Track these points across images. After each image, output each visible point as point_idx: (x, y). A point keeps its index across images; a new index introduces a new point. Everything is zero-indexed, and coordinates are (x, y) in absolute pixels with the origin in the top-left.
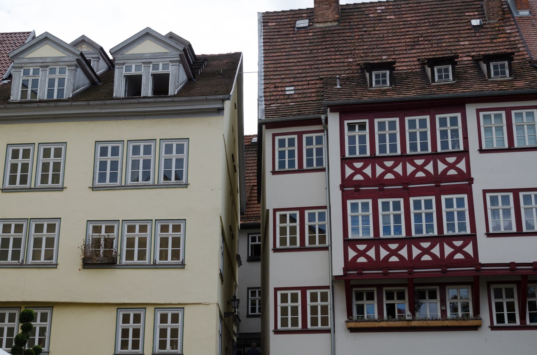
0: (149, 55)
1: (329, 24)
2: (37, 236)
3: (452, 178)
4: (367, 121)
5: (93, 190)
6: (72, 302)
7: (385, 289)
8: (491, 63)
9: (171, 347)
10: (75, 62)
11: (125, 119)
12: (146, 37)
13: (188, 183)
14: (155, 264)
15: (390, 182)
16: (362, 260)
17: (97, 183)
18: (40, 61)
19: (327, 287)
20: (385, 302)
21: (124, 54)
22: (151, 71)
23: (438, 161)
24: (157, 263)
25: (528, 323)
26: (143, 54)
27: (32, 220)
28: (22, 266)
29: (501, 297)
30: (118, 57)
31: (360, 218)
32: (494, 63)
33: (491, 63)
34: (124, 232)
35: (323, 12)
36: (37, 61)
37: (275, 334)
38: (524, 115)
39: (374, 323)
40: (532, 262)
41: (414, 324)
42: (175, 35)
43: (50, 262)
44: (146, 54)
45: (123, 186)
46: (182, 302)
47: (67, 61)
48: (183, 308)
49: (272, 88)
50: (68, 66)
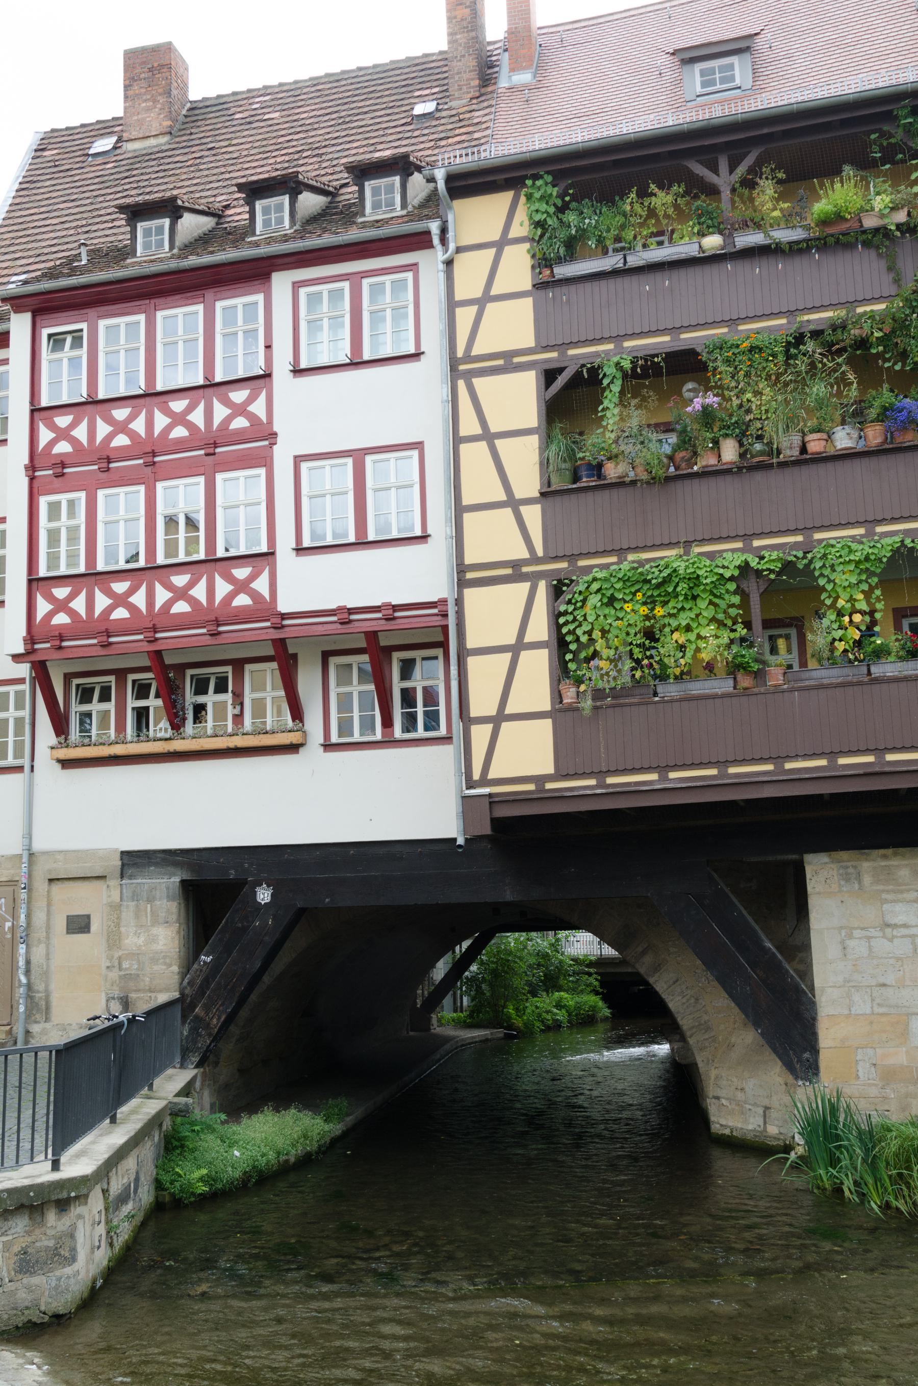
1: (153, 142)
3: (241, 437)
4: (84, 326)
7: (131, 677)
8: (367, 183)
15: (124, 454)
16: (61, 619)
19: (21, 681)
20: (132, 703)
23: (215, 401)
25: (398, 733)
29: (350, 683)
31: (64, 533)
32: (372, 182)
33: (367, 183)
35: (140, 116)
38: (388, 286)
39: (101, 747)
40: (379, 604)
41: (178, 745)
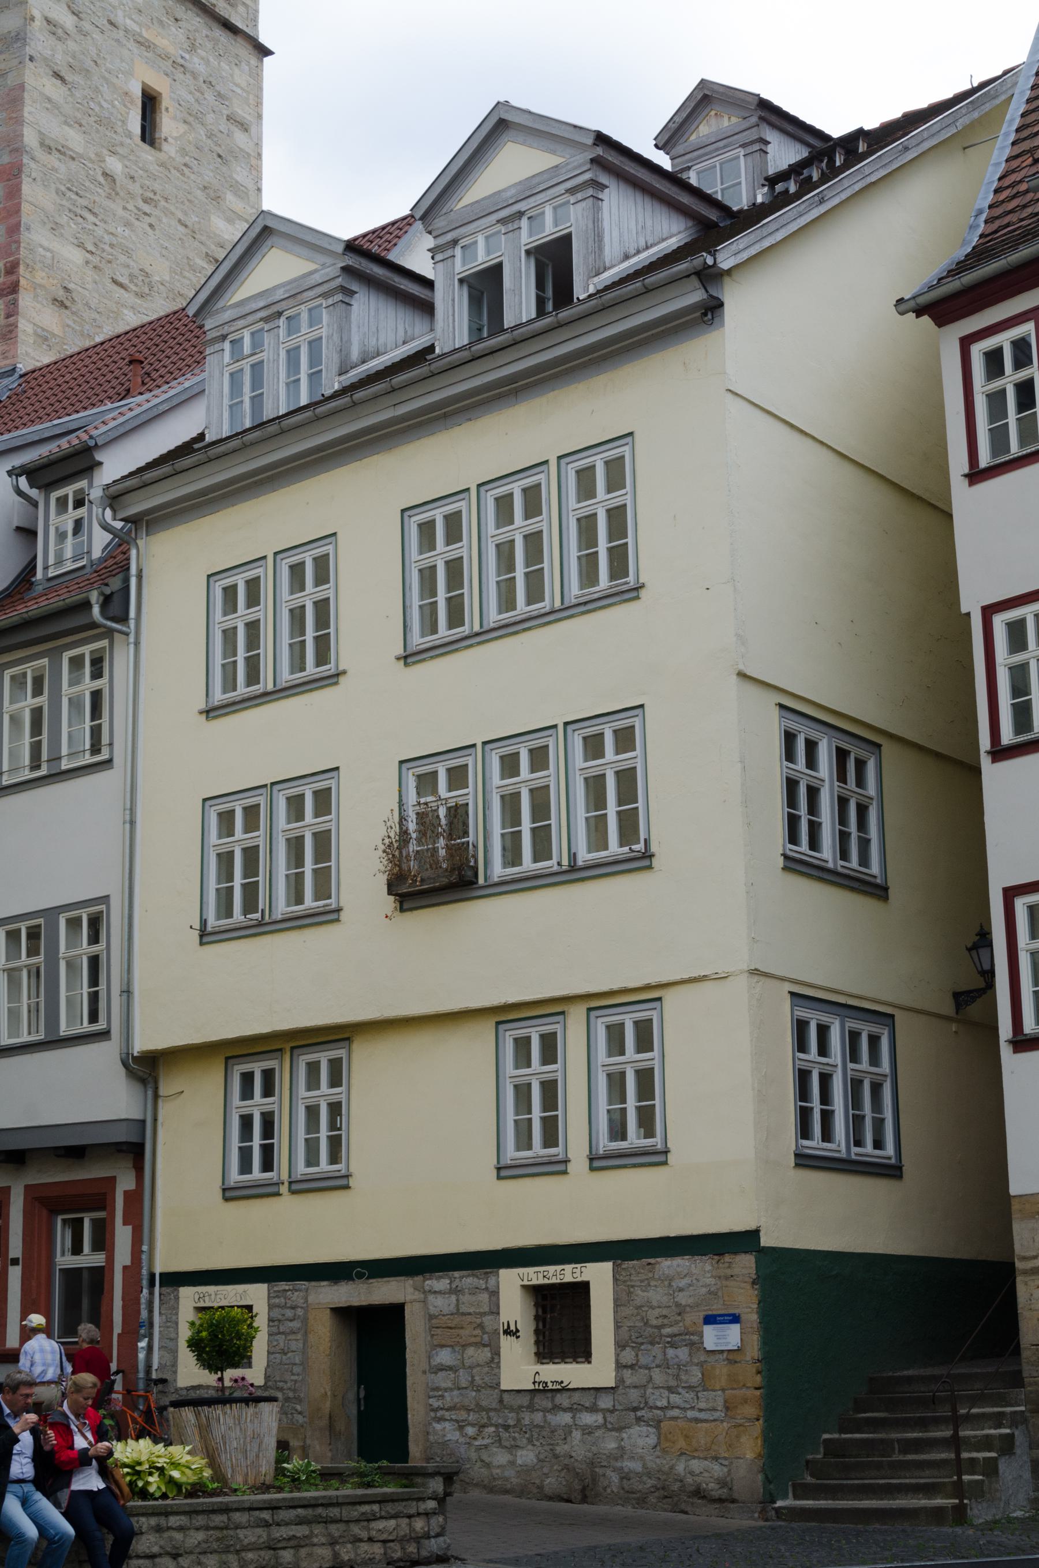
0: (513, 191)
2: (292, 832)
5: (406, 664)
6: (382, 1018)
9: (642, 1130)
10: (340, 279)
11: (470, 420)
12: (504, 135)
13: (641, 581)
14: (573, 868)
17: (417, 640)
18: (261, 304)
21: (451, 211)
22: (527, 237)
24: (580, 863)
26: (499, 192)
27: (276, 787)
28: (262, 928)
30: (436, 226)
34: (491, 778)
36: (255, 306)
37: (1016, 1051)
42: (716, 87)
43: (323, 906)
44: (504, 190)
45: (477, 634)
46: (653, 980)
47: (320, 281)
48: (659, 999)
49: (1026, 166)
50: (325, 295)
